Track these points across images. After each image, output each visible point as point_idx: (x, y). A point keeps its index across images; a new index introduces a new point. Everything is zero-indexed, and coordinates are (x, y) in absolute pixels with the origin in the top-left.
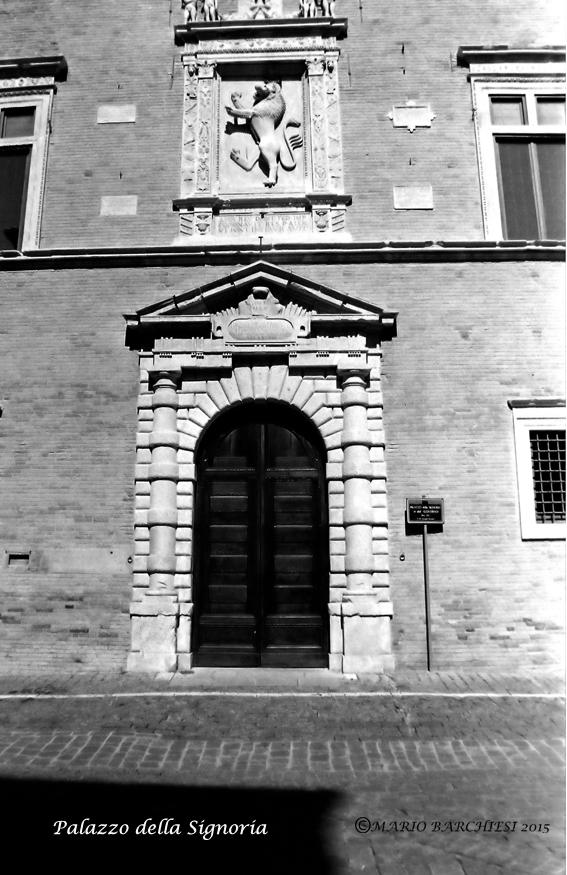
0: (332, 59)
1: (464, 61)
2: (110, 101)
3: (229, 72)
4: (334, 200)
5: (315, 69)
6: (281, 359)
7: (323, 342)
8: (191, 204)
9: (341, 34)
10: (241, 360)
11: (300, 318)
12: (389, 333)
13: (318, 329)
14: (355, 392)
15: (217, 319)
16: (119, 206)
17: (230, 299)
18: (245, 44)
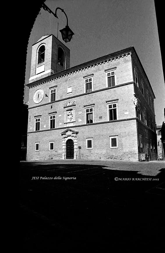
0: (74, 108)
1: (84, 107)
2: (60, 114)
3: (68, 110)
4: (74, 122)
5: (73, 109)
6: (70, 136)
7: (73, 134)
8: (65, 123)
9: (75, 106)
10: (68, 136)
11: (72, 132)
12: (78, 133)
13: (73, 133)
14: (75, 138)
15: (66, 133)
16: (60, 124)
17: (67, 132)
18: (68, 108)
